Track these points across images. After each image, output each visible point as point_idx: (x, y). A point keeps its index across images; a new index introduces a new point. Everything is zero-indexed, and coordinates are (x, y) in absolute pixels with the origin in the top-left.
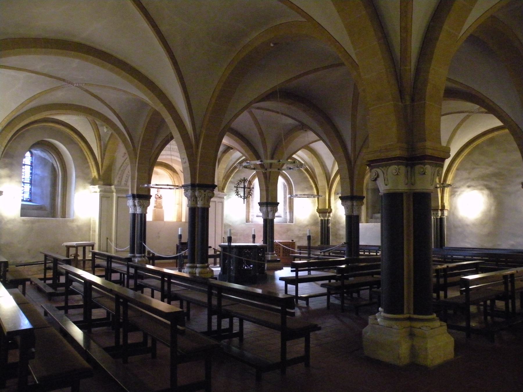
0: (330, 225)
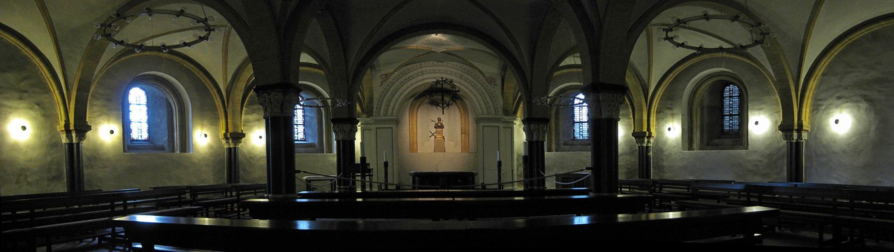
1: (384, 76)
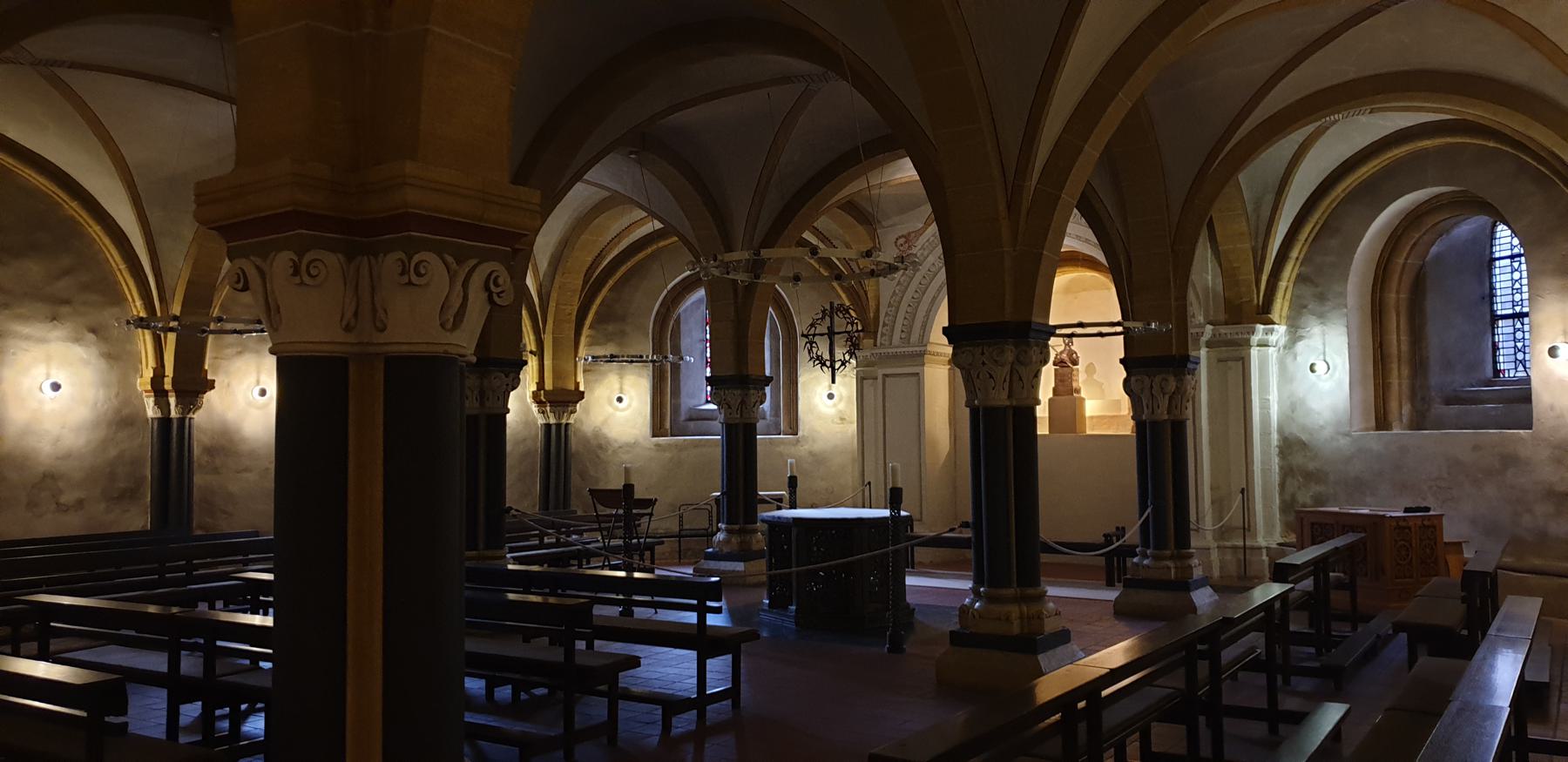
1: (901, 241)
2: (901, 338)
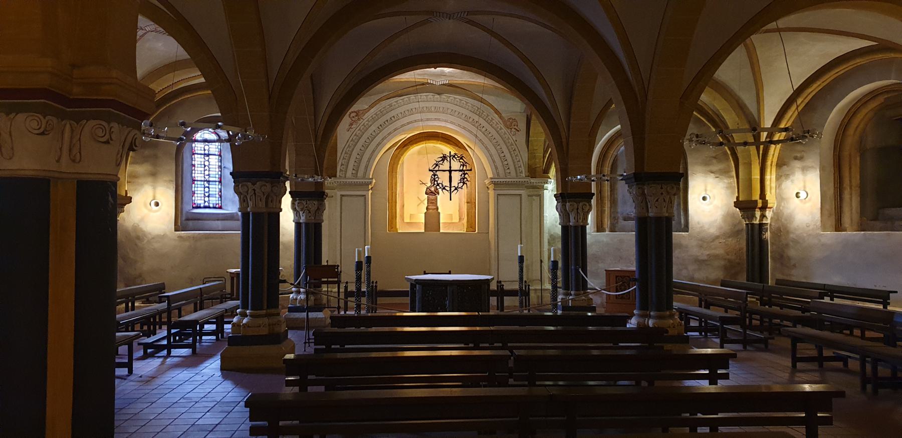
0: (768, 235)
2: (352, 174)
